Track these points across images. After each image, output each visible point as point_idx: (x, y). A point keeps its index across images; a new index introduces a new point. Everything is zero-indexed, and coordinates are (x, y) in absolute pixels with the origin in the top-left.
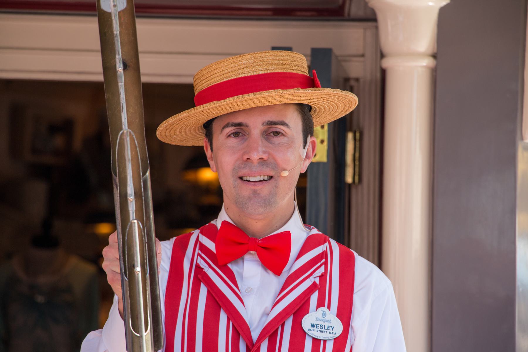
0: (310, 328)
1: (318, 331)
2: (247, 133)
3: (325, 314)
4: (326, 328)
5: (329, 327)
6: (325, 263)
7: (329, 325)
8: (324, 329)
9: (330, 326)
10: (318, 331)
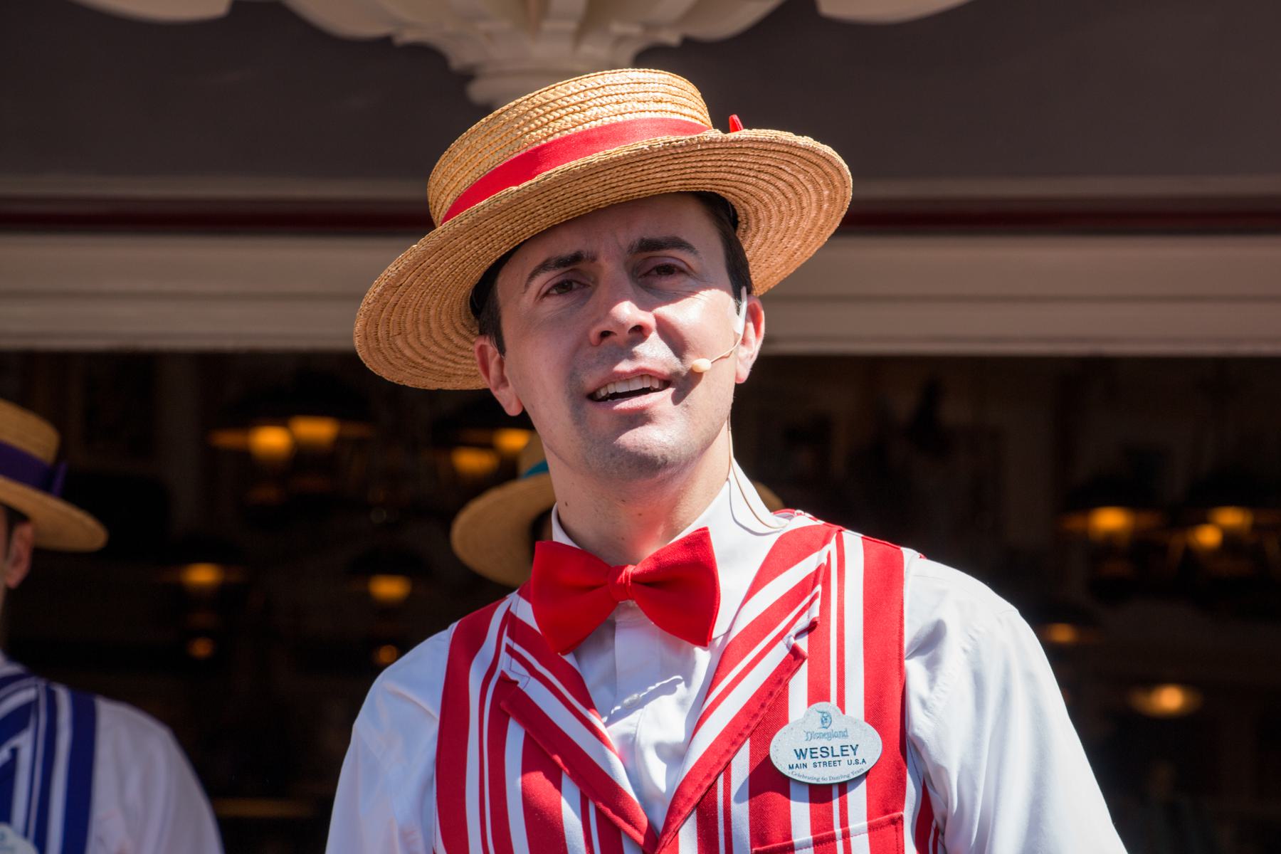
0: (794, 760)
1: (818, 765)
2: (592, 279)
3: (828, 718)
4: (837, 752)
5: (844, 748)
6: (807, 590)
7: (842, 745)
8: (833, 756)
9: (847, 746)
10: (818, 765)
